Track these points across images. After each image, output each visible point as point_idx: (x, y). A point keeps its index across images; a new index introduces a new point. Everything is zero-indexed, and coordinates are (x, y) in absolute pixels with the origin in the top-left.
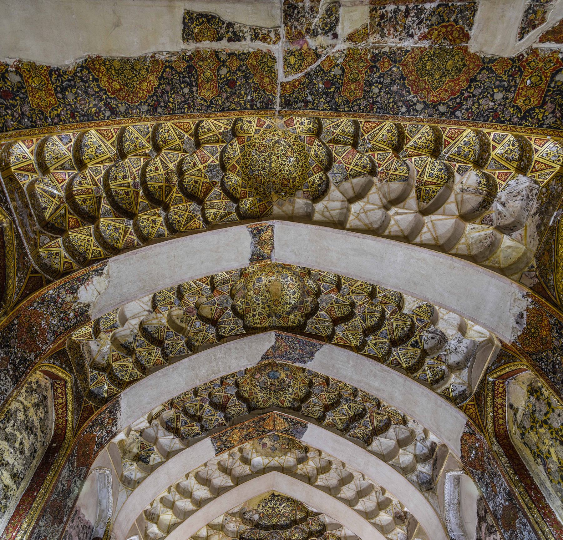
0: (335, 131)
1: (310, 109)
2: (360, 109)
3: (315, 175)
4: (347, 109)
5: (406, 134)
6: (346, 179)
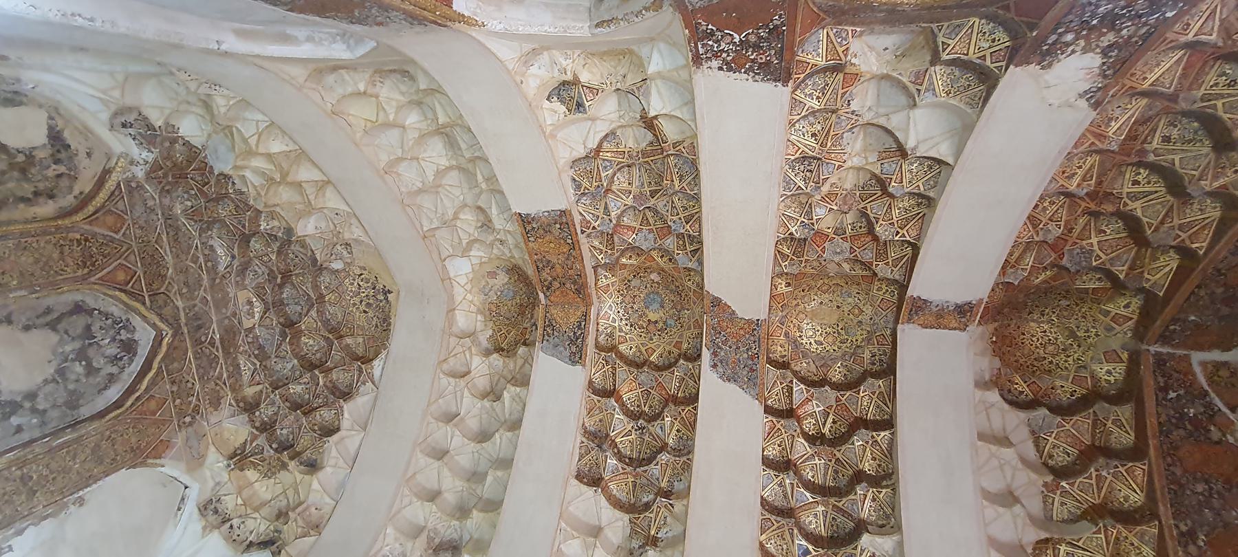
0: (1110, 422)
1: (1157, 395)
2: (1169, 465)
3: (1025, 386)
4: (1165, 447)
5: (1139, 528)
6: (1033, 432)
